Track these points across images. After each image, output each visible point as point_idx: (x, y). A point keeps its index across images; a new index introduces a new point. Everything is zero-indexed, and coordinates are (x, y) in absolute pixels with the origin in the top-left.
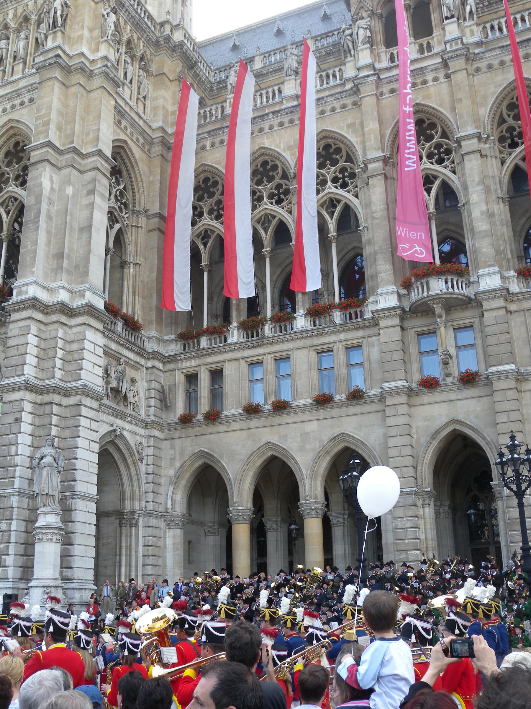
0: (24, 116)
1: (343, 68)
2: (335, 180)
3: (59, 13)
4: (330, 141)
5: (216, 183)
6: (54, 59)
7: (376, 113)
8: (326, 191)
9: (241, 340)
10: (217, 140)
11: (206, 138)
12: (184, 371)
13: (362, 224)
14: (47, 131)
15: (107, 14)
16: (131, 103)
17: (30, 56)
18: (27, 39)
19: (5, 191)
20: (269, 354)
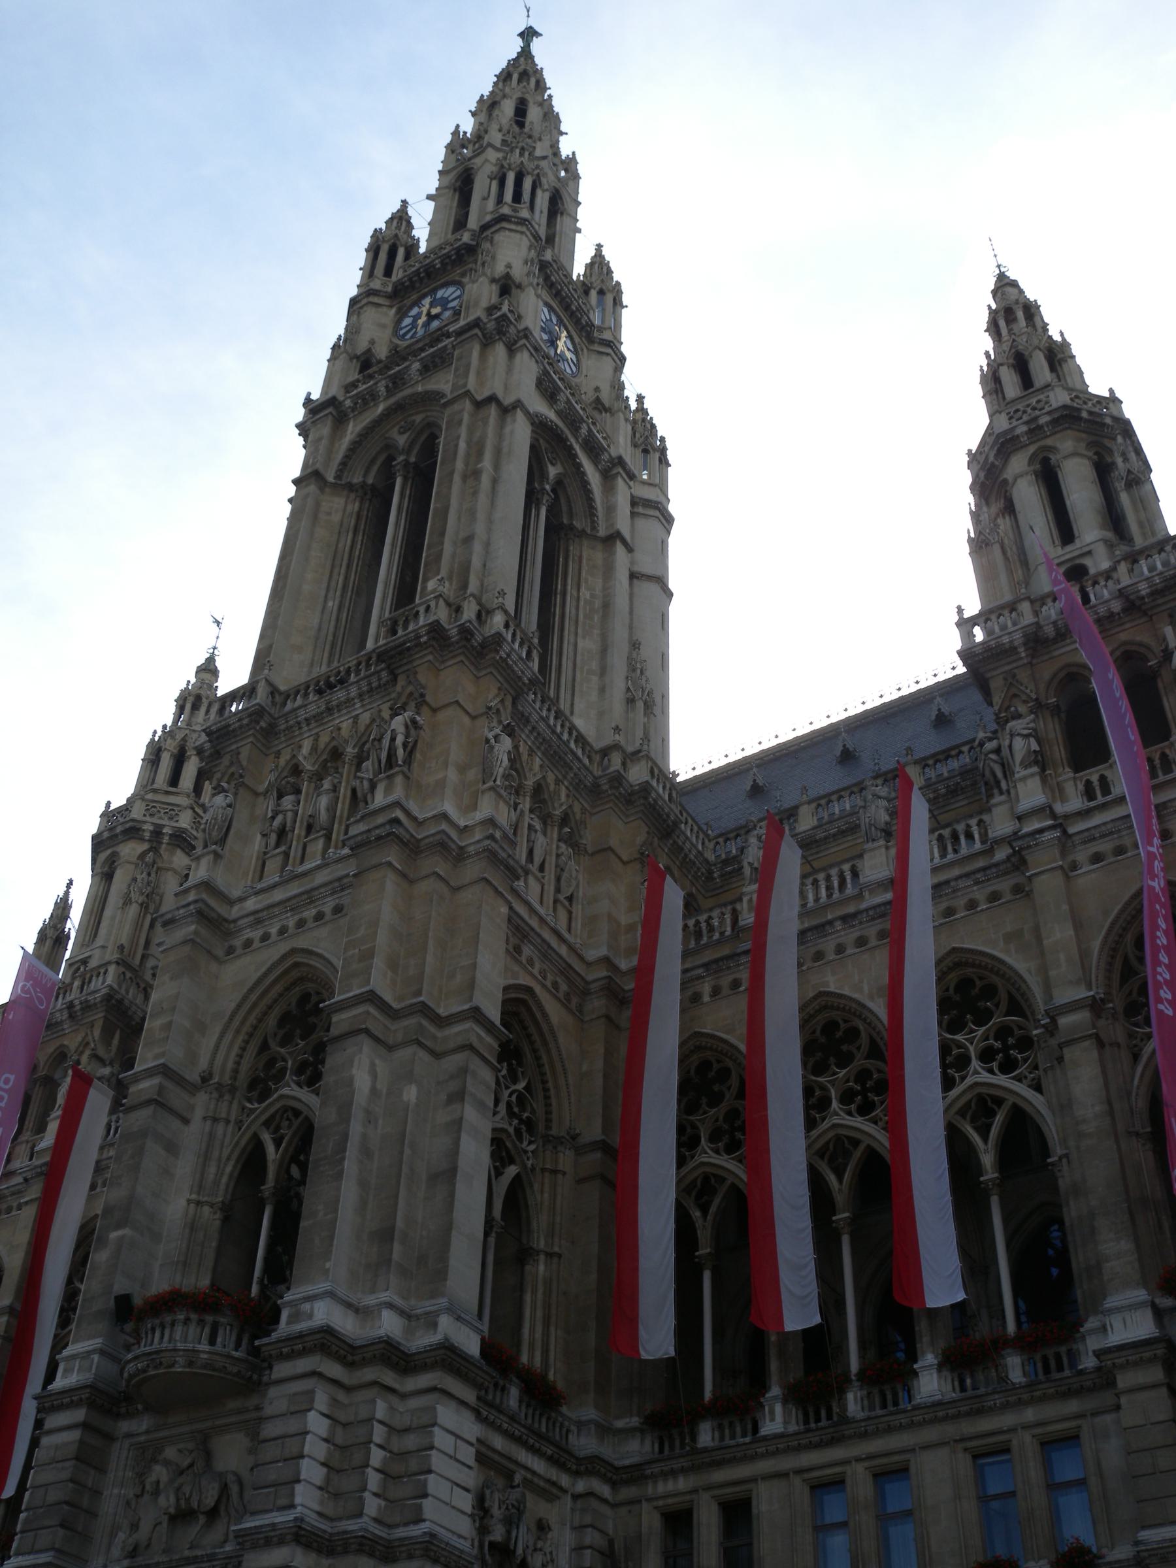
0: (323, 942)
1: (985, 817)
2: (986, 1056)
3: (400, 739)
4: (969, 971)
5: (725, 1074)
6: (388, 827)
7: (1065, 907)
8: (969, 1081)
9: (793, 1428)
10: (726, 981)
11: (699, 977)
12: (661, 1503)
13: (1057, 1150)
14: (367, 972)
15: (496, 737)
16: (542, 911)
17: (340, 823)
18: (335, 791)
19: (275, 1096)
20: (859, 1460)
